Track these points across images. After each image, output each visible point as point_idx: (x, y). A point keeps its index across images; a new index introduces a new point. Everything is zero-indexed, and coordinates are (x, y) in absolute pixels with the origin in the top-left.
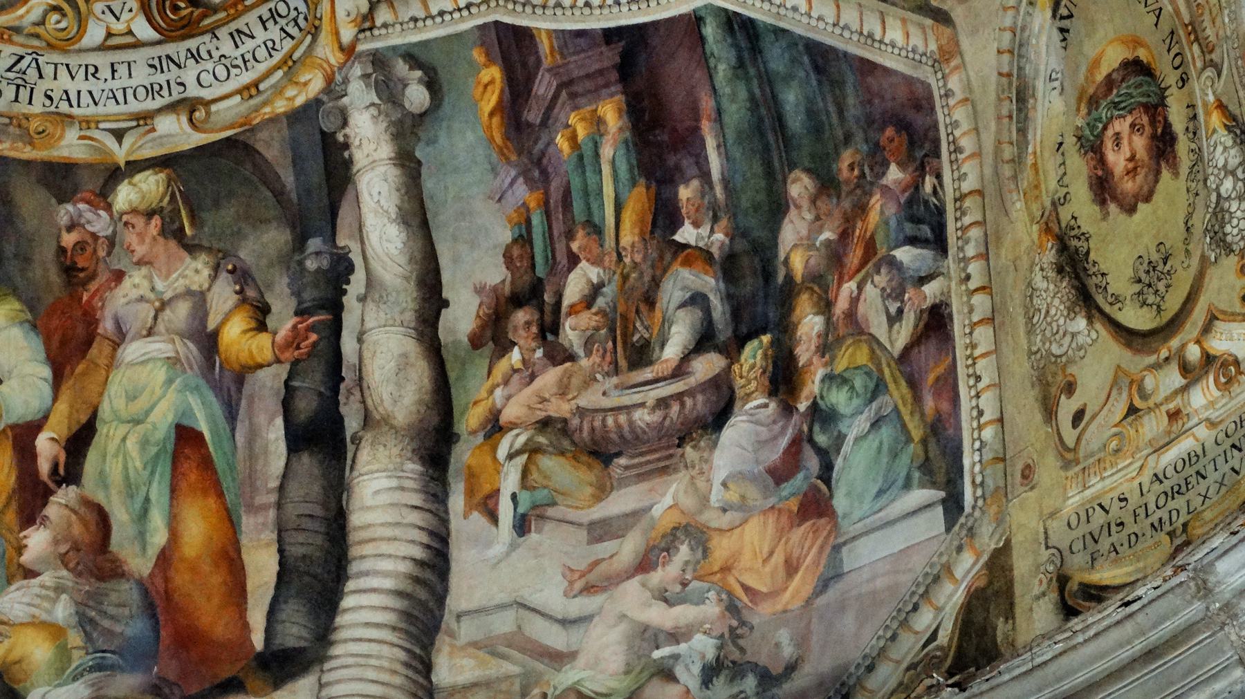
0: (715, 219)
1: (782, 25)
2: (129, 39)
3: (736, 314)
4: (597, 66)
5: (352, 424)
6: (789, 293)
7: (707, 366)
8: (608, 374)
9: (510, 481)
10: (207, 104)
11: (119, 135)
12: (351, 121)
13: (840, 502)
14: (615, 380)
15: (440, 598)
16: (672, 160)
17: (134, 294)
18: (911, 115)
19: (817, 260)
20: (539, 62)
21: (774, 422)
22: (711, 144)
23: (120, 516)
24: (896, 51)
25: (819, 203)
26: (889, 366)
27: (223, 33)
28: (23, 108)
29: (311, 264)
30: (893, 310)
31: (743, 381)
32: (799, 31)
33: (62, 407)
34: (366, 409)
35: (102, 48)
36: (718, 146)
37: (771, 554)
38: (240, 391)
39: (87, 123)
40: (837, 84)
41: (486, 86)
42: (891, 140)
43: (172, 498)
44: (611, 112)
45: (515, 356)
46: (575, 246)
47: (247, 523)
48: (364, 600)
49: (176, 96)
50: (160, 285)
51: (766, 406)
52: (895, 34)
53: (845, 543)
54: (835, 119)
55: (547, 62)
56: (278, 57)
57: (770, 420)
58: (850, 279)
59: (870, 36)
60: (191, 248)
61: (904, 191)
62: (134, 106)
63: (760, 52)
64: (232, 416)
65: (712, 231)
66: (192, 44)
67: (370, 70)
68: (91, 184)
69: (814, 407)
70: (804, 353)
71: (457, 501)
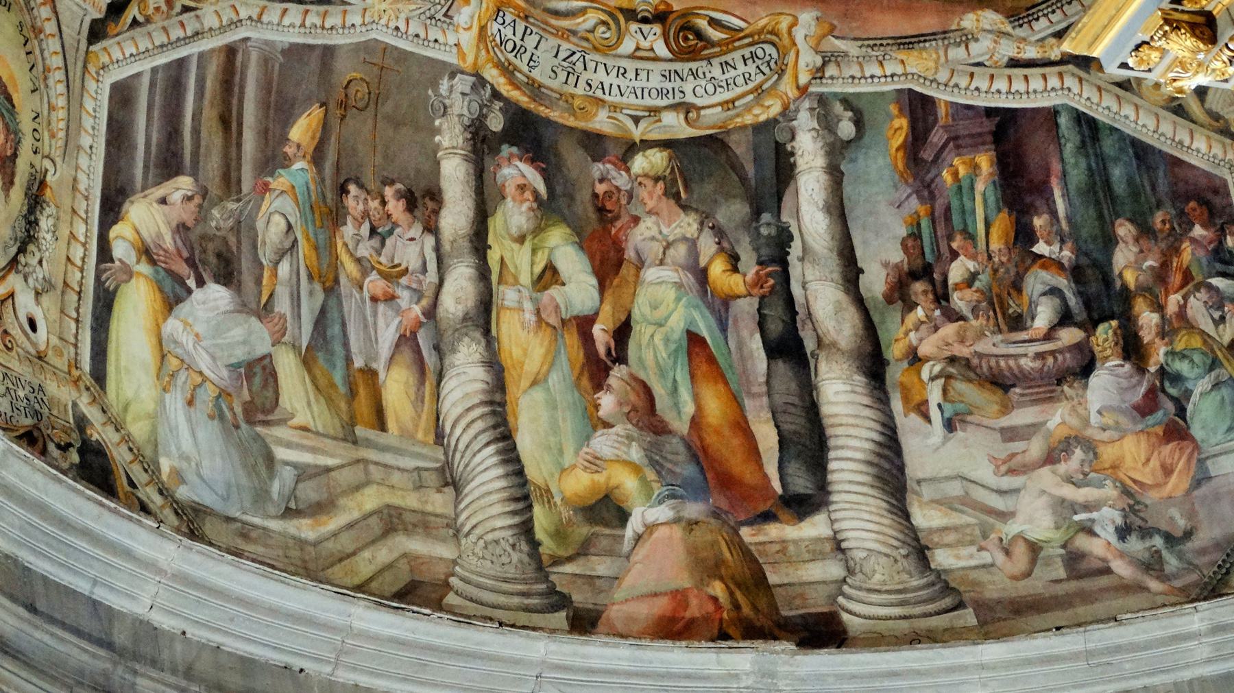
0: (1062, 241)
1: (1116, 125)
2: (651, 54)
3: (1087, 304)
4: (979, 130)
5: (810, 345)
6: (1126, 296)
7: (1070, 336)
8: (993, 333)
9: (934, 395)
10: (699, 109)
11: (636, 120)
12: (798, 138)
13: (1197, 431)
14: (1000, 337)
15: (901, 468)
16: (1028, 199)
17: (648, 234)
18: (1210, 196)
19: (1145, 278)
20: (936, 121)
21: (1131, 377)
22: (1057, 193)
23: (659, 390)
24: (1200, 155)
25: (1141, 242)
26: (1220, 350)
27: (716, 62)
28: (570, 89)
29: (764, 231)
30: (1217, 315)
31: (1100, 348)
32: (1127, 131)
33: (607, 308)
34: (818, 337)
35: (632, 57)
36: (1063, 195)
37: (1148, 460)
38: (727, 310)
39: (615, 108)
40: (1150, 169)
41: (896, 130)
42: (1194, 210)
43: (692, 382)
44: (985, 161)
45: (920, 312)
46: (955, 245)
47: (748, 404)
48: (843, 465)
49: (677, 100)
50: (665, 231)
51: (1122, 366)
52: (1200, 143)
53: (1208, 458)
54: (1148, 188)
55: (941, 122)
56: (751, 85)
57: (1127, 375)
58: (1176, 292)
59: (1181, 143)
60: (685, 208)
61: (1210, 243)
62: (648, 102)
63: (1098, 140)
64: (724, 328)
65: (1061, 249)
66: (693, 65)
67: (816, 106)
68: (615, 151)
69: (1162, 372)
70: (1147, 335)
71: (897, 405)
